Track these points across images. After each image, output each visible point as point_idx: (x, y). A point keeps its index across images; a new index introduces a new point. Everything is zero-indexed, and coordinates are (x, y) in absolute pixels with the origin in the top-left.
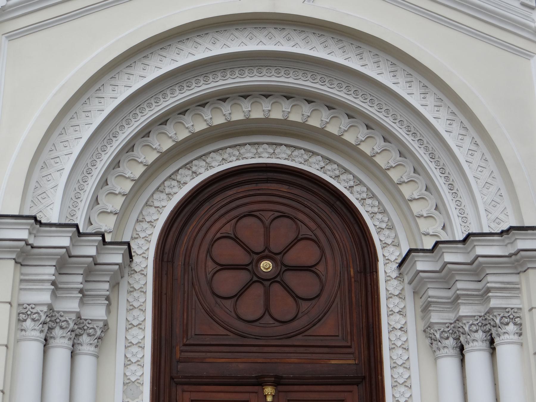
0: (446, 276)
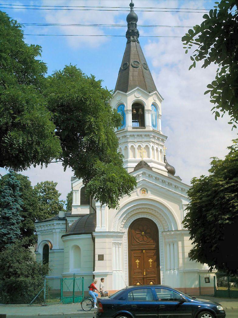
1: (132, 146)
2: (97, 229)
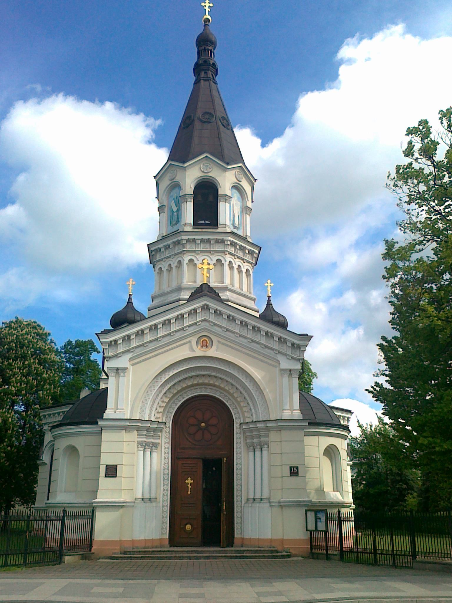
0: (250, 430)
1: (191, 261)
2: (109, 414)
